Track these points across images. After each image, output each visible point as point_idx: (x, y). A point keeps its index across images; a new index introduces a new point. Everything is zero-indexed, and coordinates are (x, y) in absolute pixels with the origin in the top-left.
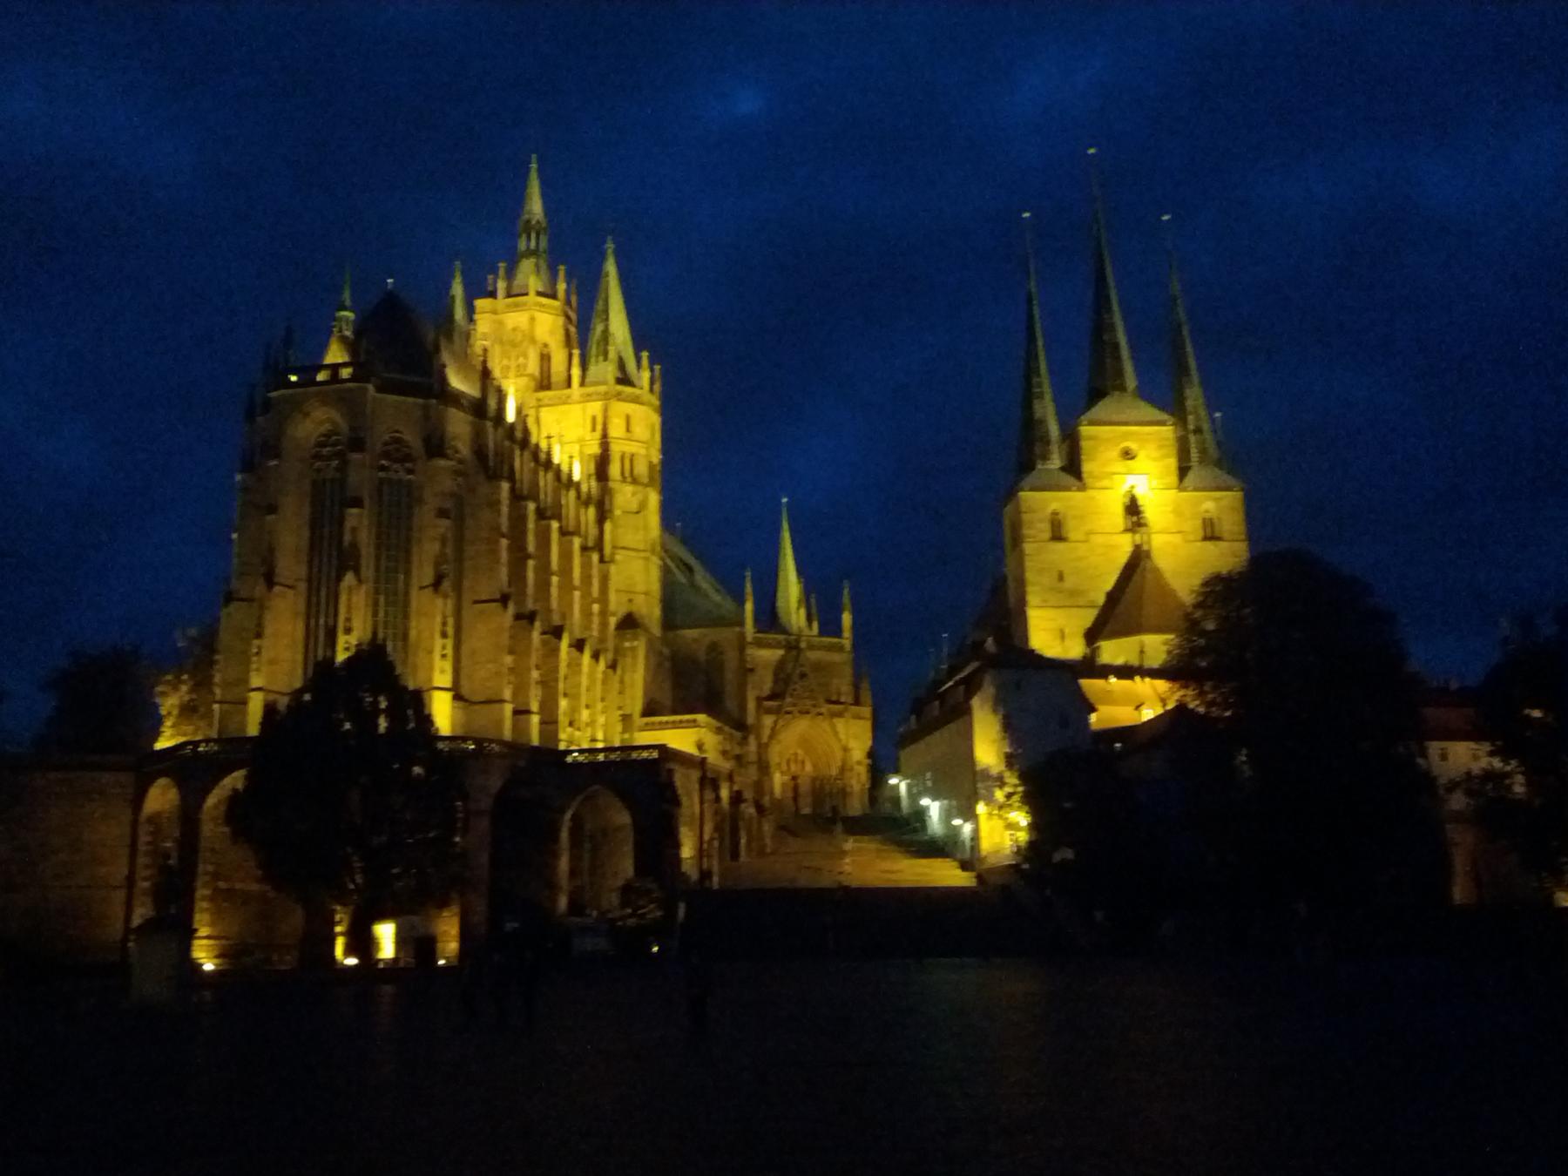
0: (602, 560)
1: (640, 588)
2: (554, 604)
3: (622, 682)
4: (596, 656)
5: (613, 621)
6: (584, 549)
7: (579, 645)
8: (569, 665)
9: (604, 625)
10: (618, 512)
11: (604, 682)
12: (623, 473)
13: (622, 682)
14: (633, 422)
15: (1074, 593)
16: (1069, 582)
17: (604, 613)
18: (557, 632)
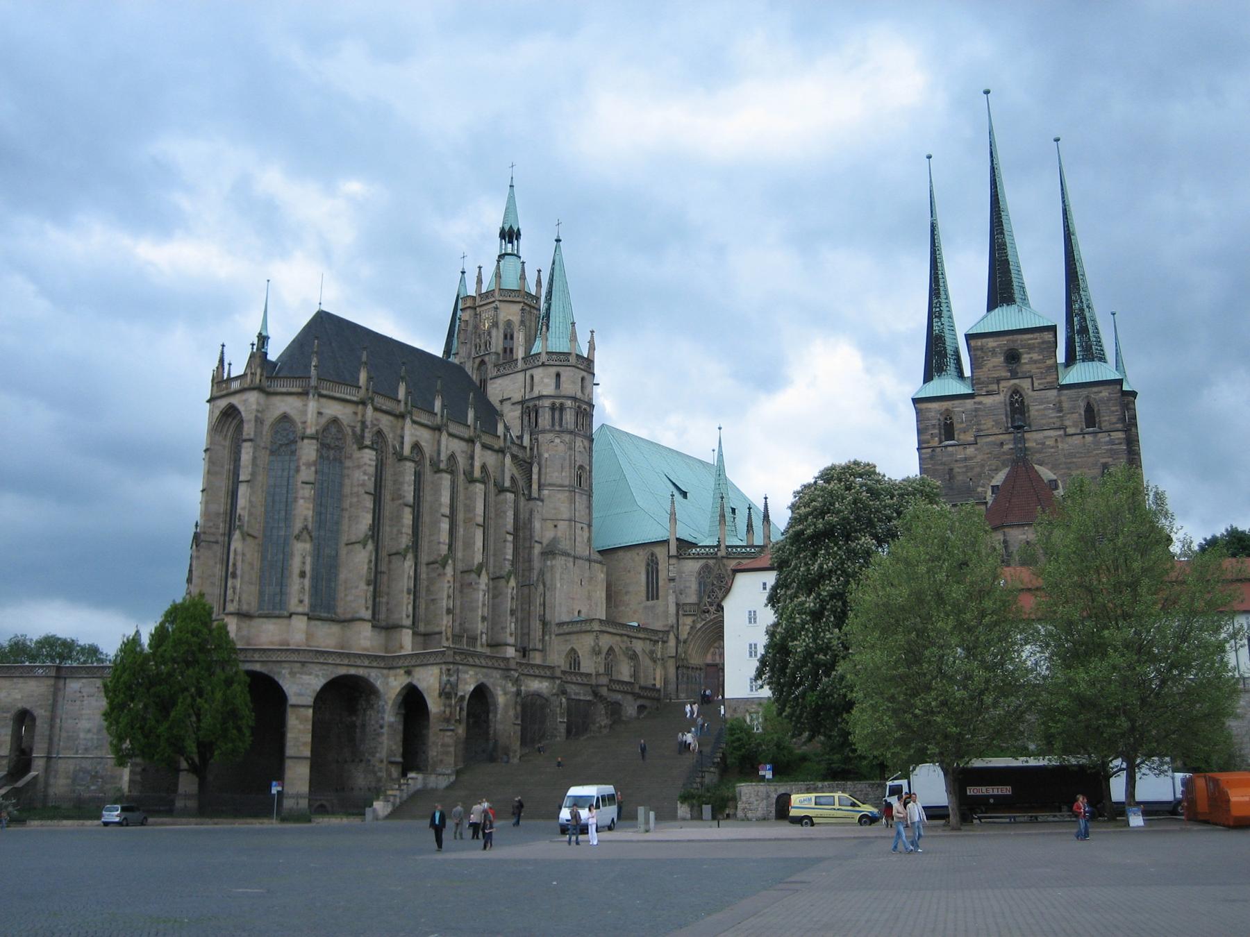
1: (566, 516)
5: (537, 549)
10: (546, 455)
12: (553, 425)
14: (563, 379)
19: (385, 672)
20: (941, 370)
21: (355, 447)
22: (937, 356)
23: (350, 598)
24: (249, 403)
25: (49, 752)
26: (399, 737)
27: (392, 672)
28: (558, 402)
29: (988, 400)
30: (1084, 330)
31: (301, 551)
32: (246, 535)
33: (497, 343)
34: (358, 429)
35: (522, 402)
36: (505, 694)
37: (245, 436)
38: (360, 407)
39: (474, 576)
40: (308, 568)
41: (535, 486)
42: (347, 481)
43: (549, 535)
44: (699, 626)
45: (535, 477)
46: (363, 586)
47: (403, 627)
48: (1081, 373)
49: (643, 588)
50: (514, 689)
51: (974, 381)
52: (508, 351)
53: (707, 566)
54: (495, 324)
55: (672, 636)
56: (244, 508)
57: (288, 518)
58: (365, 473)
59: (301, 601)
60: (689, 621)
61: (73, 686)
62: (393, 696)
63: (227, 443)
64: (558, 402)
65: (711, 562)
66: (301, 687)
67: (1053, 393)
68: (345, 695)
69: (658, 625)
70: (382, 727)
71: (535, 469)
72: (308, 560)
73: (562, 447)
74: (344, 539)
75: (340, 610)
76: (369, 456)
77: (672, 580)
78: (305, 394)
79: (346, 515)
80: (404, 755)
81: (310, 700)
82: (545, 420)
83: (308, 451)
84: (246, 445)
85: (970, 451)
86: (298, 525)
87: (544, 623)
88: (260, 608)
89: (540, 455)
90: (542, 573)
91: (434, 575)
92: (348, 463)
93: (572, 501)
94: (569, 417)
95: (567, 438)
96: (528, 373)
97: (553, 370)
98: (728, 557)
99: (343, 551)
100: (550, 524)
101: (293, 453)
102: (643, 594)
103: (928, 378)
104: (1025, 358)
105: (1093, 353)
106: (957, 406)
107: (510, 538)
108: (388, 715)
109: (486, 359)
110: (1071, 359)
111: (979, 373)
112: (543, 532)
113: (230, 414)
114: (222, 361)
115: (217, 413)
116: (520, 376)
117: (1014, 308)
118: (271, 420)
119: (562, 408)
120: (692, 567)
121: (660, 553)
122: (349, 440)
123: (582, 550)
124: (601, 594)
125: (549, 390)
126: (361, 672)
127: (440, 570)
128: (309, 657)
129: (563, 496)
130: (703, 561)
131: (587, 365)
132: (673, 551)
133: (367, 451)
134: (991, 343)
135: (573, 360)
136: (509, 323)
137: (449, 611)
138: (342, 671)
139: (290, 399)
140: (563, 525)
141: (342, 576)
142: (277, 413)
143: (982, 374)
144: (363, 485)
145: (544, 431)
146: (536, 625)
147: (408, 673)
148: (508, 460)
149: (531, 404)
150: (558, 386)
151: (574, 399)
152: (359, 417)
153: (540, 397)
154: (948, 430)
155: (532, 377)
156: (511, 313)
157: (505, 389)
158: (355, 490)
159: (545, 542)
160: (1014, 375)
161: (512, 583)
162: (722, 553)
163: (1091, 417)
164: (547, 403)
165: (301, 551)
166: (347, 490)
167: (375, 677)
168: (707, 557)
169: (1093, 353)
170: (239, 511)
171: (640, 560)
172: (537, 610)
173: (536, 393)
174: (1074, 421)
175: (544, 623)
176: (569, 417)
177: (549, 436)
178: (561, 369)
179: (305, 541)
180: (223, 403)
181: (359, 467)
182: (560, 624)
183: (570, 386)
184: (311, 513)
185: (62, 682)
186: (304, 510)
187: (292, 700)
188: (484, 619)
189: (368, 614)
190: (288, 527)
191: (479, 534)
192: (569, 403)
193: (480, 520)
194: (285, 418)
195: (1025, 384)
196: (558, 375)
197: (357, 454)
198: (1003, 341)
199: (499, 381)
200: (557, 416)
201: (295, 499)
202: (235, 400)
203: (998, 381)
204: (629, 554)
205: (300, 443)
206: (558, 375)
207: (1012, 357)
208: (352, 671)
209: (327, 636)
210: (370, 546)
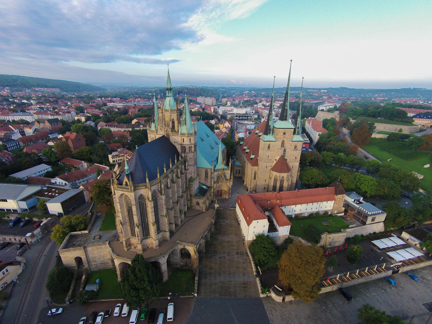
15: (270, 160)
20: (269, 133)
35: (181, 144)
39: (180, 198)
41: (187, 167)
42: (159, 202)
43: (190, 176)
45: (187, 165)
52: (173, 127)
60: (216, 185)
67: (291, 142)
71: (187, 163)
76: (163, 197)
82: (187, 150)
85: (273, 152)
87: (191, 195)
88: (144, 236)
90: (190, 185)
94: (193, 149)
95: (193, 154)
100: (190, 174)
104: (287, 134)
106: (271, 143)
108: (178, 251)
129: (193, 168)
140: (192, 174)
145: (188, 153)
146: (189, 196)
153: (186, 145)
154: (269, 147)
156: (175, 116)
157: (176, 139)
160: (284, 137)
167: (176, 248)
172: (188, 193)
175: (191, 195)
176: (193, 149)
177: (189, 154)
187: (162, 264)
195: (285, 140)
199: (174, 137)
203: (281, 138)
207: (284, 133)
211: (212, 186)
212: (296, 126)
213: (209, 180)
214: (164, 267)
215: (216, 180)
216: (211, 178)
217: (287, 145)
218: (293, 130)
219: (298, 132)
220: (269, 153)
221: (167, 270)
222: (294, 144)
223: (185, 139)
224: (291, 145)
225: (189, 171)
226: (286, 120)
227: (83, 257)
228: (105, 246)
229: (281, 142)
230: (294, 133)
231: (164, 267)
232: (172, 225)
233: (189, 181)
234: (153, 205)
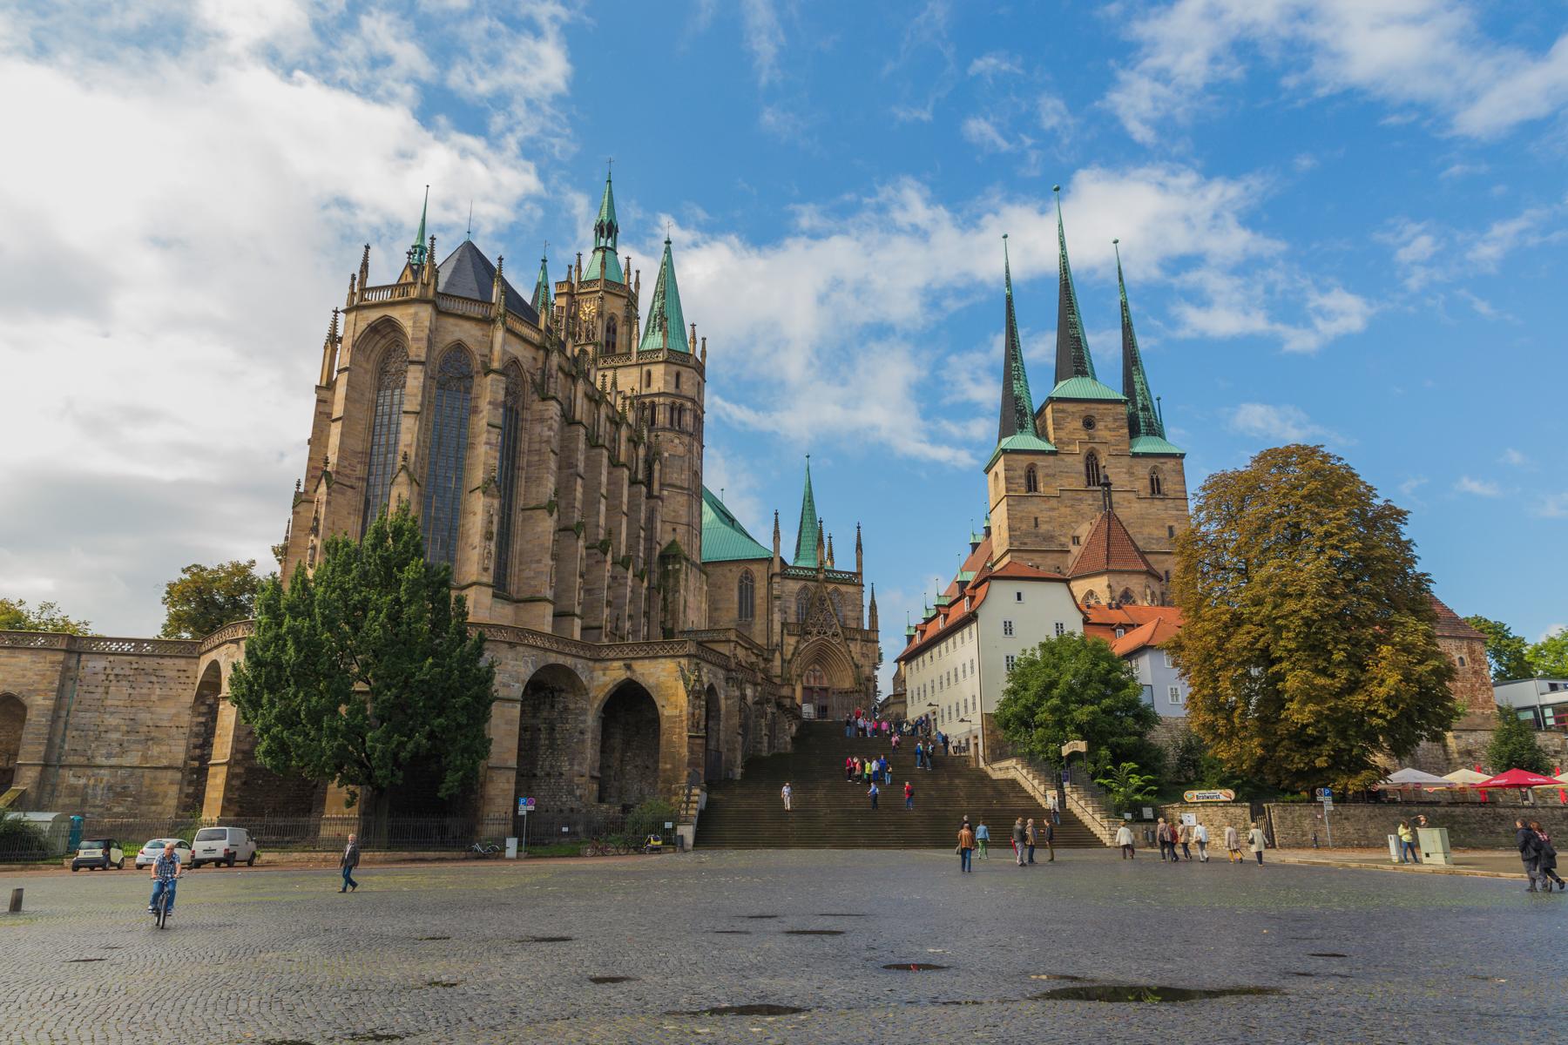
0: (650, 496)
1: (684, 520)
2: (602, 522)
3: (665, 599)
4: (639, 576)
6: (633, 482)
7: (625, 563)
8: (614, 578)
9: (649, 550)
11: (649, 599)
12: (672, 423)
13: (665, 599)
14: (683, 379)
15: (1050, 538)
16: (1044, 528)
17: (650, 539)
18: (604, 547)
19: (591, 664)
20: (1022, 427)
21: (535, 397)
22: (1014, 414)
23: (528, 573)
24: (413, 321)
25: (47, 757)
26: (598, 748)
27: (597, 665)
28: (678, 401)
29: (1069, 459)
30: (1145, 408)
31: (478, 513)
32: (412, 480)
33: (600, 336)
34: (538, 378)
36: (727, 698)
37: (412, 357)
38: (541, 352)
40: (495, 529)
41: (656, 486)
42: (525, 437)
43: (668, 538)
44: (802, 647)
45: (656, 475)
46: (548, 561)
47: (574, 615)
48: (1144, 445)
49: (736, 606)
50: (737, 693)
51: (1059, 441)
53: (805, 587)
54: (600, 314)
55: (777, 655)
56: (410, 446)
57: (460, 466)
58: (550, 429)
59: (486, 569)
61: (96, 664)
62: (601, 695)
63: (369, 367)
64: (678, 401)
65: (810, 584)
66: (512, 672)
67: (1125, 461)
68: (546, 689)
69: (760, 640)
70: (582, 733)
71: (657, 467)
72: (496, 519)
73: (681, 450)
74: (520, 502)
75: (513, 588)
77: (778, 598)
78: (488, 321)
79: (523, 474)
80: (601, 769)
81: (517, 690)
82: (662, 417)
83: (489, 391)
84: (412, 368)
85: (1054, 503)
86: (478, 476)
89: (659, 454)
90: (665, 575)
91: (592, 561)
92: (526, 415)
93: (690, 506)
95: (686, 439)
96: (645, 368)
97: (675, 368)
98: (827, 580)
99: (518, 517)
100: (668, 527)
101: (468, 390)
102: (736, 612)
103: (1005, 431)
104: (1100, 425)
105: (1155, 431)
106: (1040, 461)
107: (642, 534)
109: (590, 349)
110: (1134, 432)
111: (1062, 434)
112: (664, 537)
113: (386, 329)
114: (365, 265)
115: (362, 325)
116: (635, 372)
117: (1088, 379)
118: (441, 346)
119: (681, 409)
120: (793, 586)
121: (759, 572)
122: (528, 387)
123: (695, 558)
124: (704, 606)
125: (671, 389)
126: (569, 662)
127: (600, 556)
128: (519, 637)
129: (683, 499)
130: (802, 583)
131: (700, 369)
132: (777, 568)
133: (554, 403)
134: (1070, 407)
135: (692, 362)
136: (612, 318)
137: (609, 604)
138: (553, 659)
139: (467, 325)
140: (681, 529)
141: (517, 546)
142: (449, 339)
143: (1062, 434)
144: (548, 442)
145: (664, 429)
147: (628, 667)
148: (642, 451)
149: (647, 401)
150: (677, 386)
151: (692, 400)
152: (540, 365)
153: (659, 395)
154: (1032, 484)
155: (649, 374)
158: (537, 446)
159: (664, 544)
161: (645, 584)
162: (821, 576)
163: (1156, 486)
164: (669, 401)
165: (478, 513)
166: (524, 446)
168: (806, 578)
169: (1155, 431)
170: (401, 448)
171: (733, 577)
173: (654, 389)
174: (1143, 485)
176: (688, 419)
177: (669, 435)
178: (681, 369)
179: (493, 496)
180: (374, 315)
181: (542, 420)
182: (683, 632)
183: (687, 388)
184: (497, 463)
185: (75, 657)
186: (483, 456)
188: (630, 617)
189: (549, 594)
190: (459, 479)
191: (624, 520)
192: (689, 405)
193: (625, 508)
194: (459, 346)
196: (678, 375)
197: (538, 406)
198: (1083, 407)
200: (676, 416)
201: (472, 446)
202: (395, 313)
204: (719, 570)
205: (477, 380)
206: (678, 375)
207: (1089, 423)
208: (561, 660)
209: (504, 614)
210: (555, 515)
211: (776, 639)
212: (1134, 403)
213: (759, 626)
214: (504, 726)
215: (792, 619)
216: (771, 598)
217: (1115, 471)
218: (1123, 410)
219: (1149, 425)
220: (1034, 508)
221: (513, 763)
222: (1143, 469)
223: (658, 371)
224: (1131, 474)
225: (663, 511)
226: (1084, 374)
227: (39, 705)
228: (181, 663)
229: (1081, 458)
230: (1134, 432)
231: (504, 726)
232: (566, 621)
233: (665, 558)
234: (498, 421)
